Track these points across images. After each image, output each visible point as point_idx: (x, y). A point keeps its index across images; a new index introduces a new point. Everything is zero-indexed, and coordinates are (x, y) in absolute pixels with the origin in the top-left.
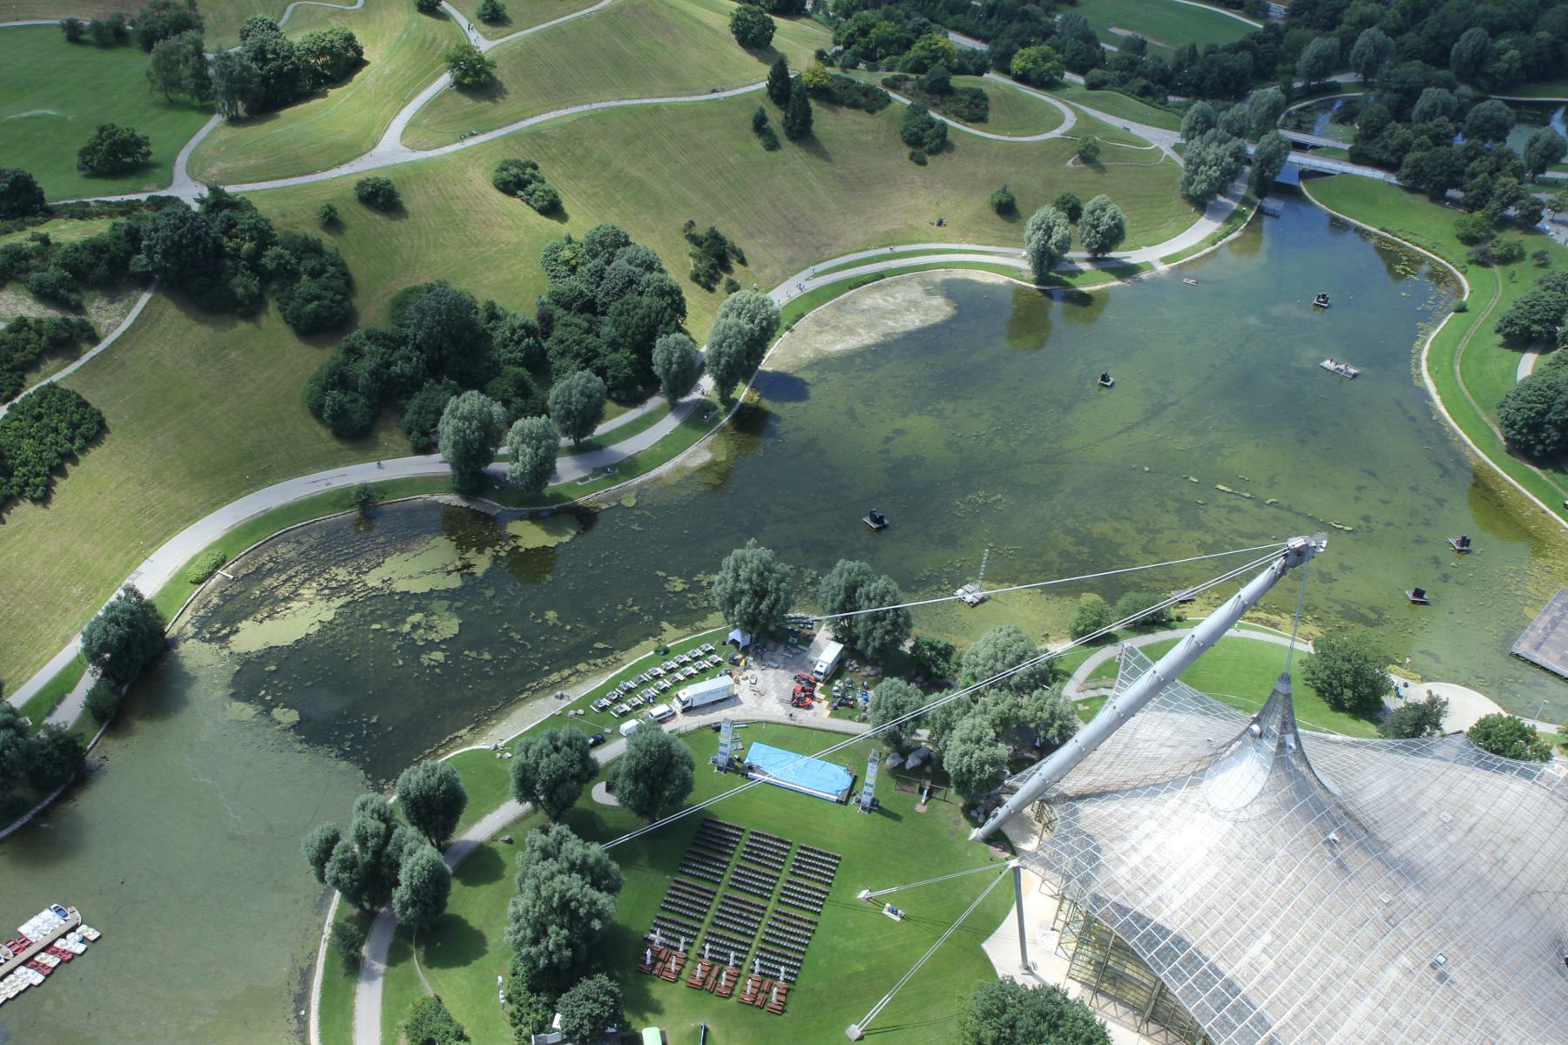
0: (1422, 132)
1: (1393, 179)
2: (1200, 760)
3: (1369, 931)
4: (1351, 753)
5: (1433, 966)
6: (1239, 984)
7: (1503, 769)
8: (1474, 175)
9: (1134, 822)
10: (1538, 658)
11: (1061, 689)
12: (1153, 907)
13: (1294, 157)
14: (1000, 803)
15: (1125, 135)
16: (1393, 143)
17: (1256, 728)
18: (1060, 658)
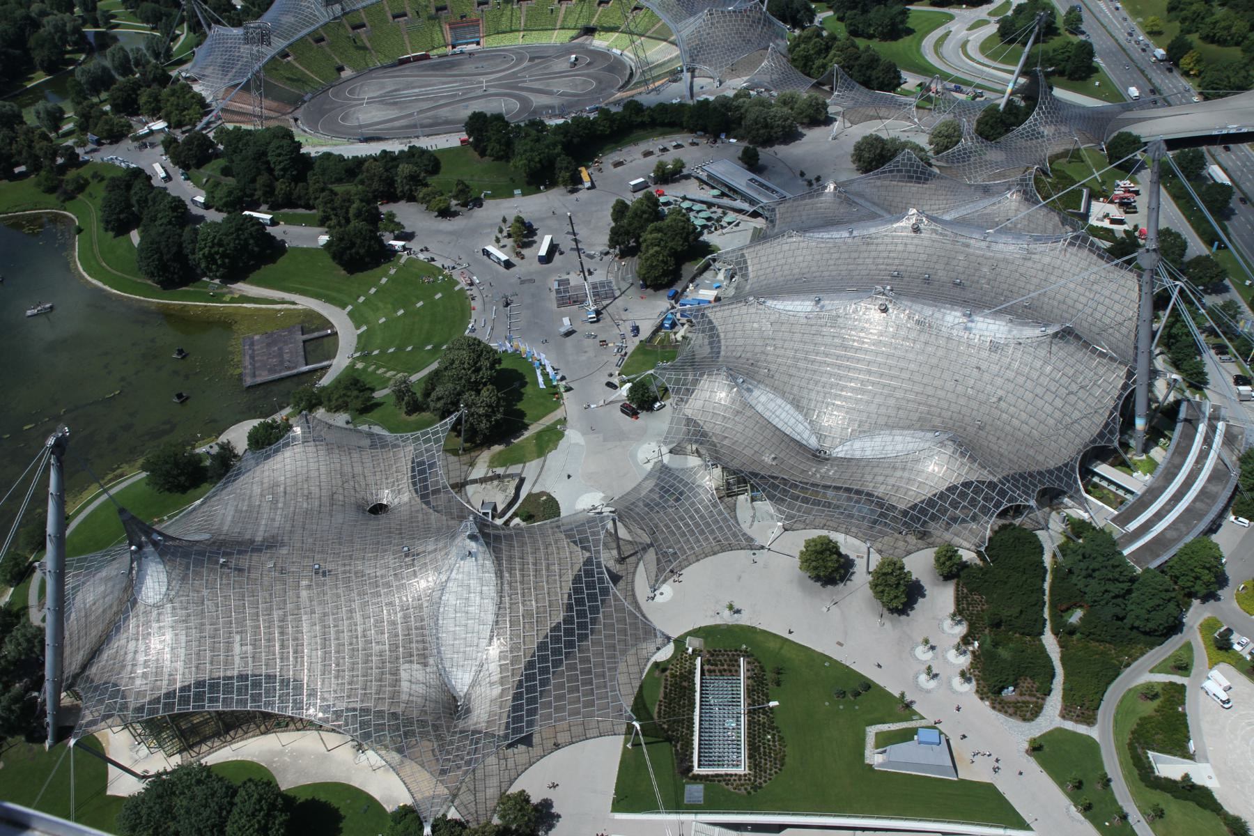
2: (125, 590)
3: (278, 587)
4: (205, 508)
5: (317, 573)
6: (244, 673)
7: (277, 451)
9: (122, 652)
10: (259, 380)
11: (28, 619)
12: (172, 681)
14: (44, 714)
17: (133, 548)
18: (10, 604)
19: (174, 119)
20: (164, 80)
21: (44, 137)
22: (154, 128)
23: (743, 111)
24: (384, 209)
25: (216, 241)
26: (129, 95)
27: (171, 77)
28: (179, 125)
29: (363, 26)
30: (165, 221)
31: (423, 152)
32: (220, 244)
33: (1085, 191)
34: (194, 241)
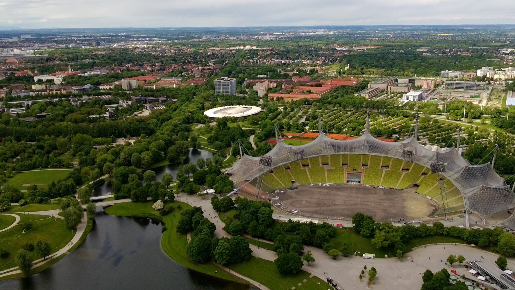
0: (132, 185)
1: (129, 200)
8: (152, 192)
13: (98, 204)
15: (40, 217)
16: (126, 190)
19: (218, 190)
20: (219, 172)
21: (163, 187)
22: (208, 192)
23: (499, 238)
24: (307, 249)
25: (226, 247)
26: (202, 177)
27: (221, 172)
28: (220, 192)
29: (308, 165)
30: (206, 233)
31: (330, 226)
32: (227, 249)
34: (216, 244)
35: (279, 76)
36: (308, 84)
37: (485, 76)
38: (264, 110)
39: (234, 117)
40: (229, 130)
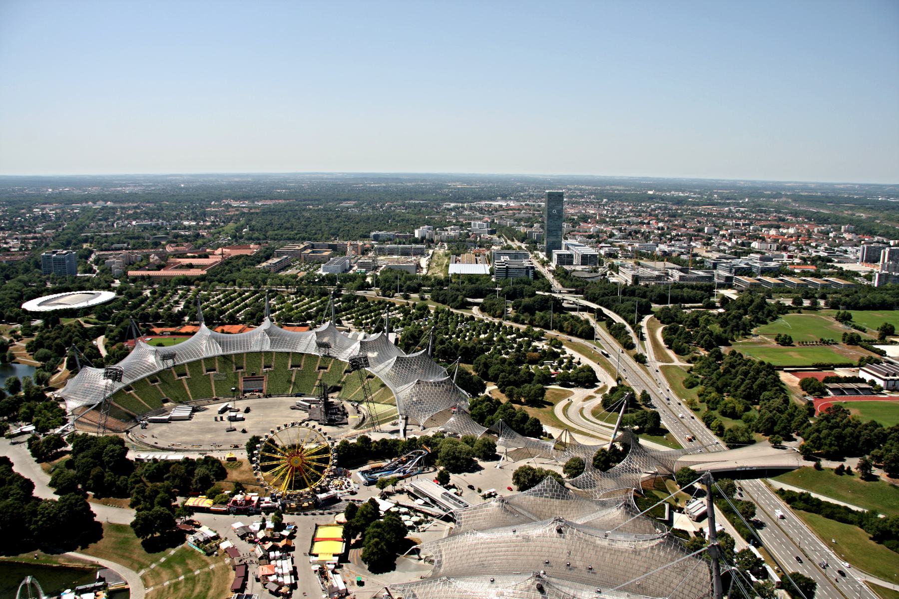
20: (42, 397)
23: (439, 446)
27: (46, 396)
29: (185, 374)
33: (667, 506)
35: (145, 245)
36: (189, 254)
37: (423, 238)
38: (121, 297)
39: (71, 309)
40: (62, 330)
